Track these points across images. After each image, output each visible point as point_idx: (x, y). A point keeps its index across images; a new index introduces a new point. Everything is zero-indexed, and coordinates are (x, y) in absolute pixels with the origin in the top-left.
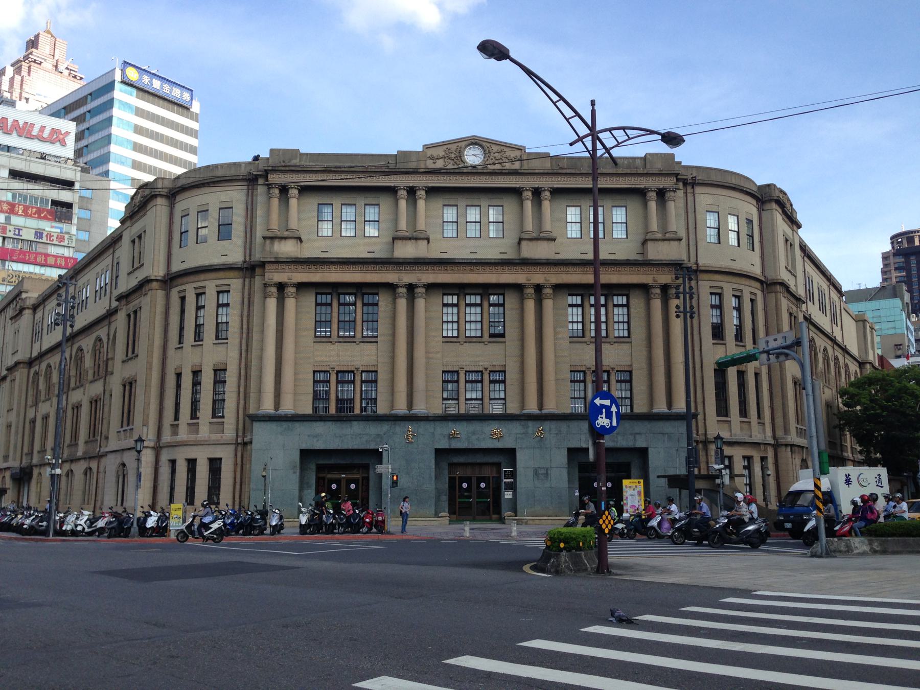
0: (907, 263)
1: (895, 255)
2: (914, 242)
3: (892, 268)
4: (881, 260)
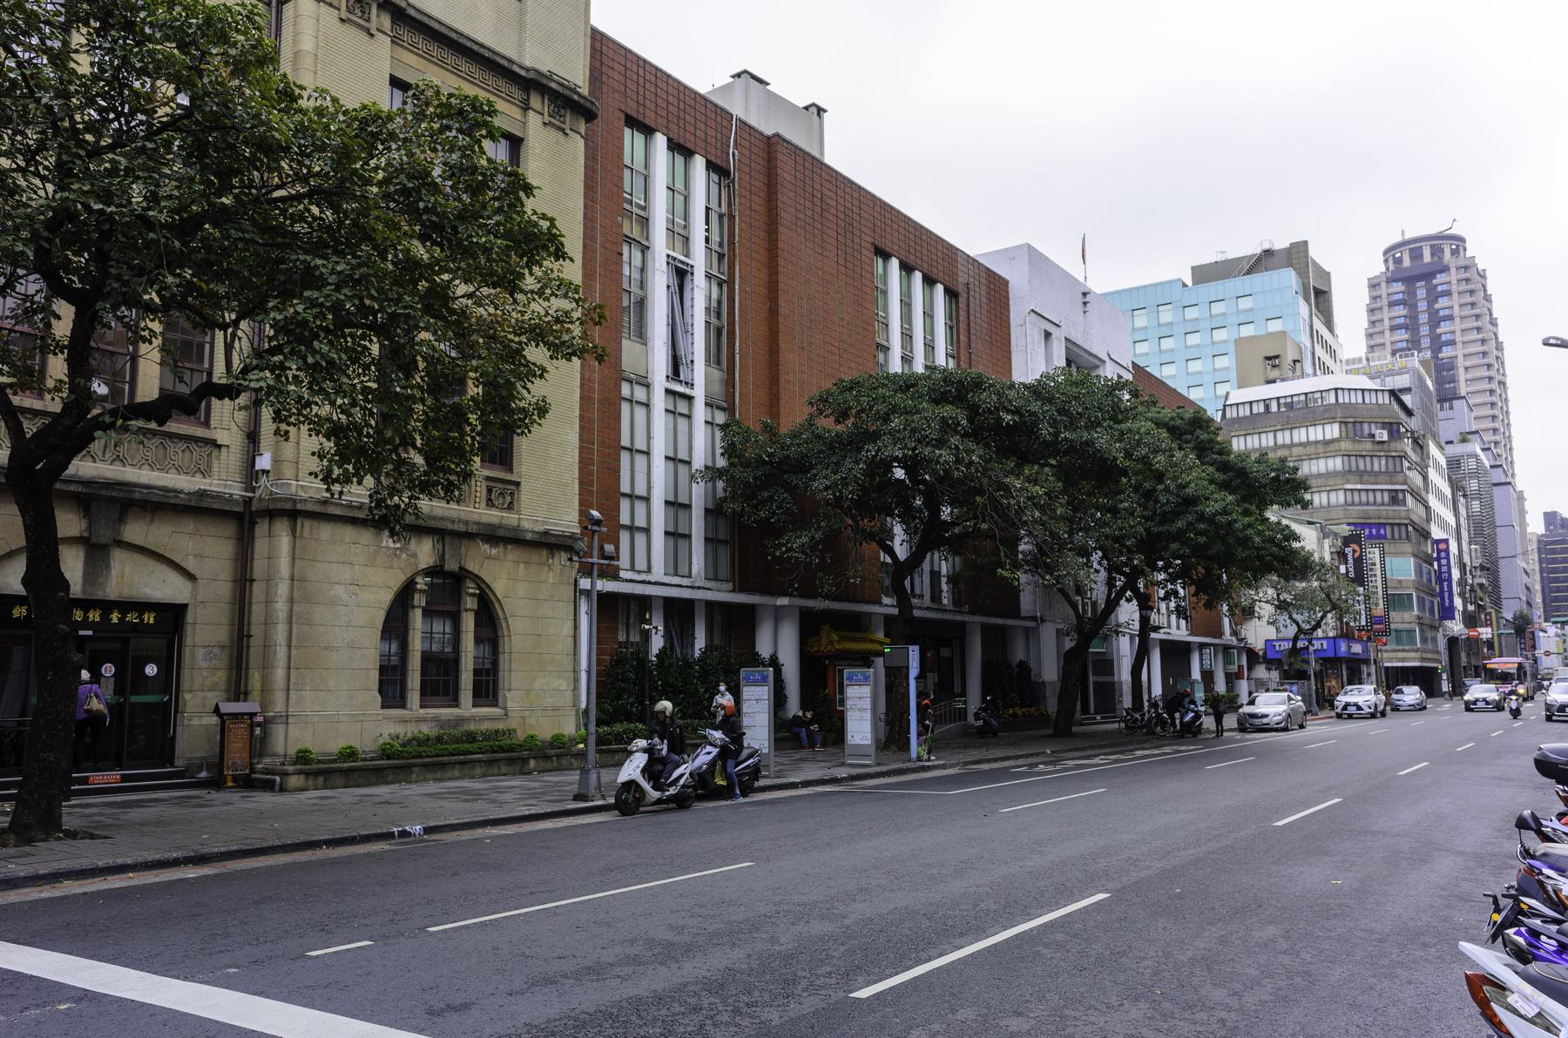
0: (1411, 293)
1: (1389, 281)
2: (1421, 256)
3: (1385, 302)
4: (1366, 290)
